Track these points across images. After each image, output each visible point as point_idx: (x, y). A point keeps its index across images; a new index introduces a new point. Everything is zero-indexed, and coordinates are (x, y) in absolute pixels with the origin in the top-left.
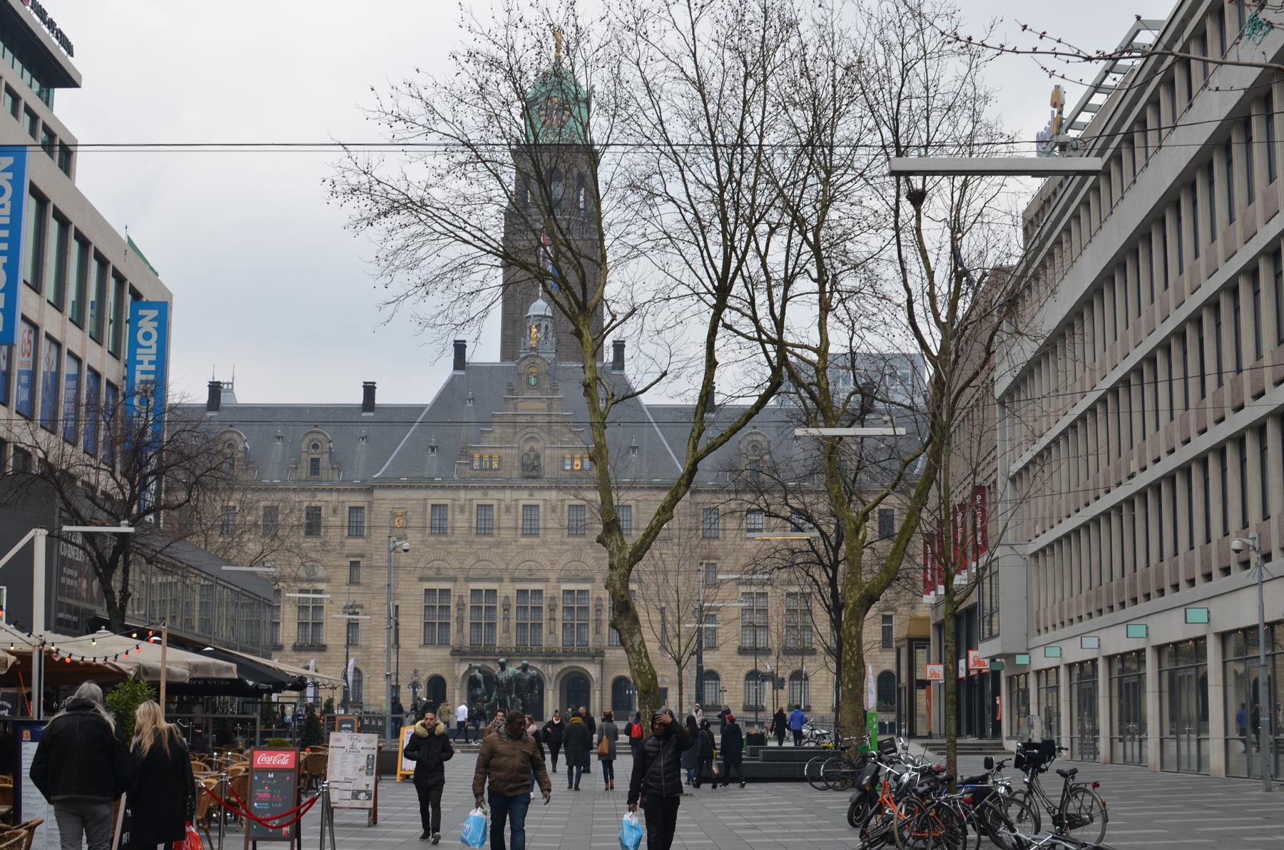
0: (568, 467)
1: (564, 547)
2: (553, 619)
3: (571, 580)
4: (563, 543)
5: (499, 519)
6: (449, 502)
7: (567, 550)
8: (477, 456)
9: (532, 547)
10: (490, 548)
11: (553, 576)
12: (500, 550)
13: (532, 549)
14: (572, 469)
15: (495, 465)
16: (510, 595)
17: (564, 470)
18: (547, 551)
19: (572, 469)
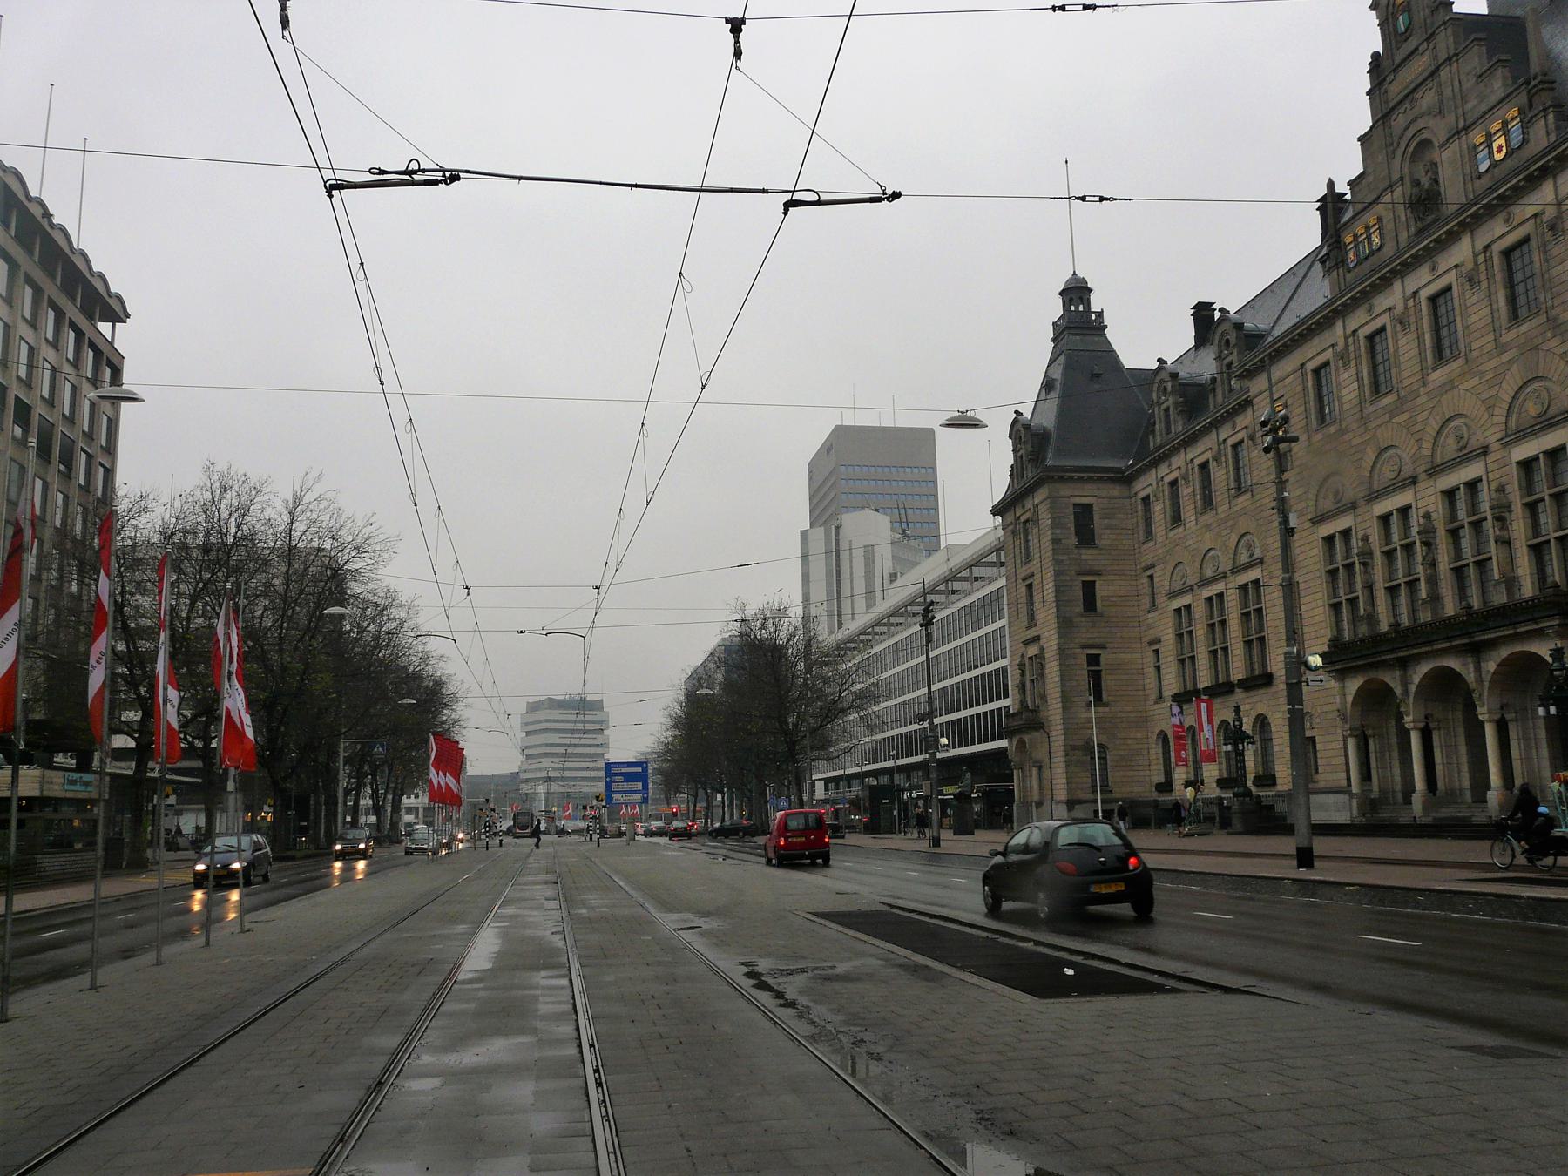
0: (1483, 167)
1: (1505, 357)
2: (1506, 542)
3: (1523, 434)
4: (1500, 348)
5: (1397, 349)
6: (1328, 354)
7: (1511, 361)
8: (1349, 239)
9: (1450, 386)
10: (1391, 418)
11: (1493, 436)
12: (1406, 416)
13: (1453, 388)
14: (1494, 165)
15: (1376, 240)
16: (1432, 508)
17: (1480, 176)
18: (1475, 381)
19: (1494, 165)
